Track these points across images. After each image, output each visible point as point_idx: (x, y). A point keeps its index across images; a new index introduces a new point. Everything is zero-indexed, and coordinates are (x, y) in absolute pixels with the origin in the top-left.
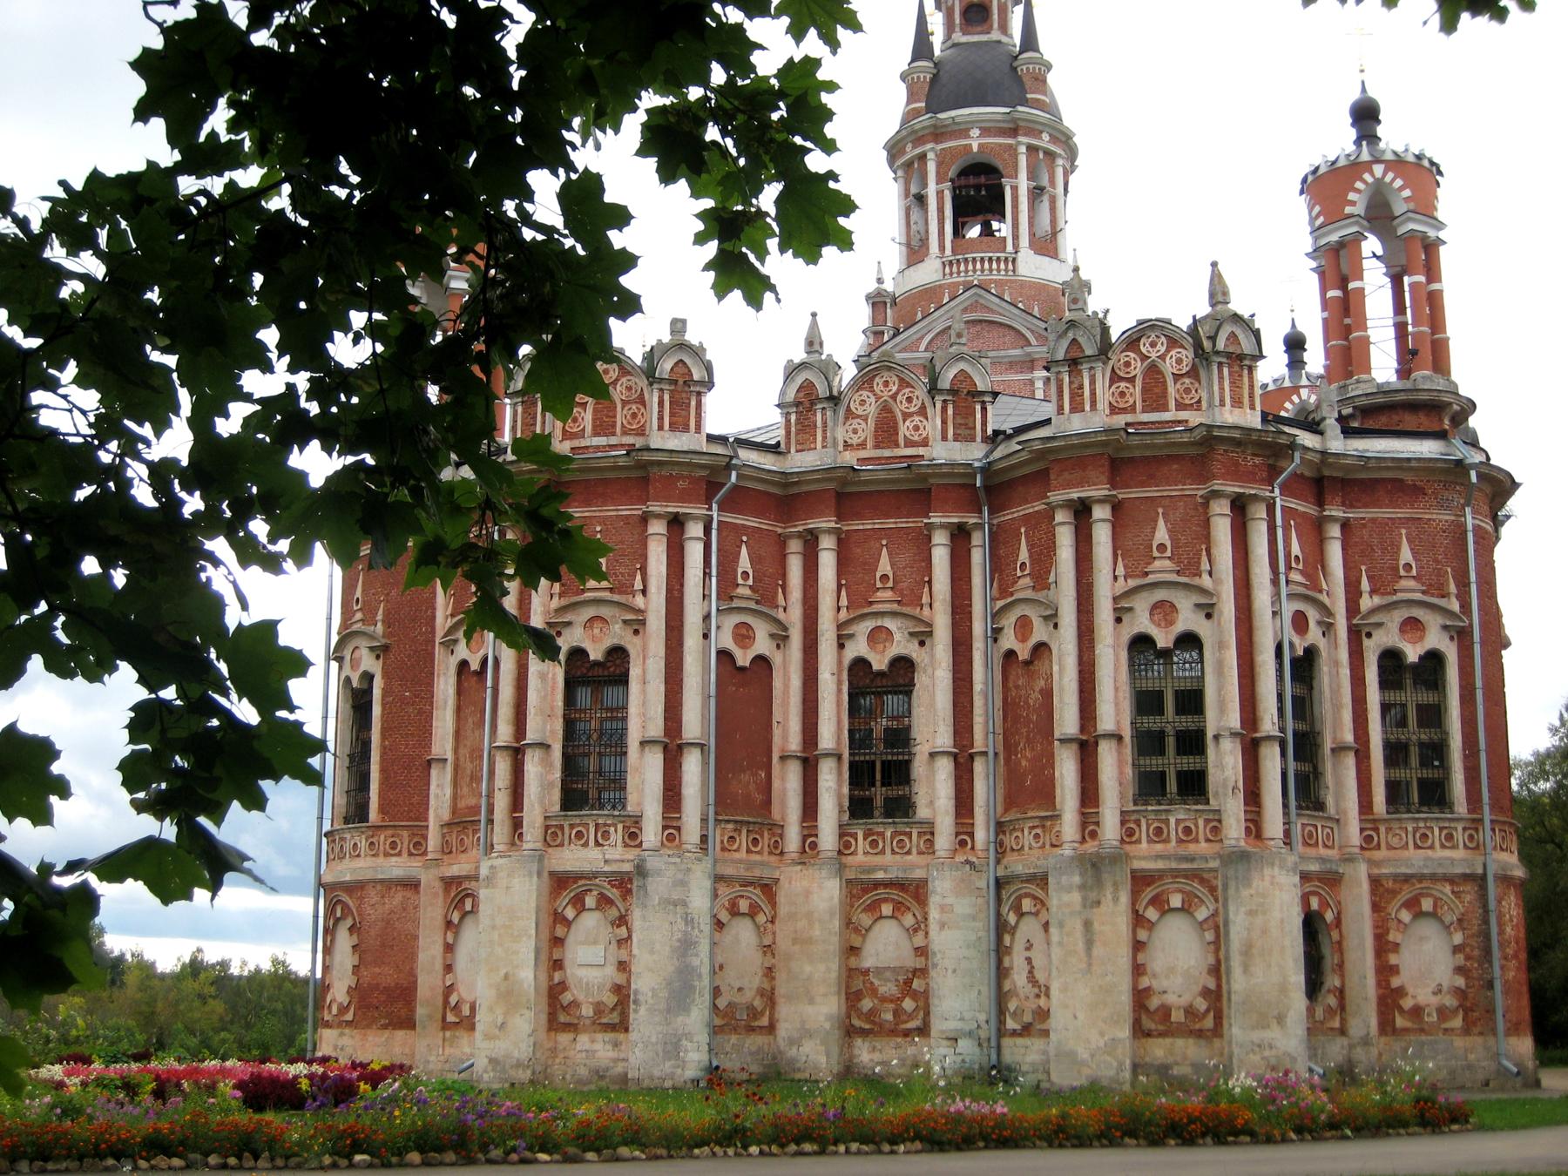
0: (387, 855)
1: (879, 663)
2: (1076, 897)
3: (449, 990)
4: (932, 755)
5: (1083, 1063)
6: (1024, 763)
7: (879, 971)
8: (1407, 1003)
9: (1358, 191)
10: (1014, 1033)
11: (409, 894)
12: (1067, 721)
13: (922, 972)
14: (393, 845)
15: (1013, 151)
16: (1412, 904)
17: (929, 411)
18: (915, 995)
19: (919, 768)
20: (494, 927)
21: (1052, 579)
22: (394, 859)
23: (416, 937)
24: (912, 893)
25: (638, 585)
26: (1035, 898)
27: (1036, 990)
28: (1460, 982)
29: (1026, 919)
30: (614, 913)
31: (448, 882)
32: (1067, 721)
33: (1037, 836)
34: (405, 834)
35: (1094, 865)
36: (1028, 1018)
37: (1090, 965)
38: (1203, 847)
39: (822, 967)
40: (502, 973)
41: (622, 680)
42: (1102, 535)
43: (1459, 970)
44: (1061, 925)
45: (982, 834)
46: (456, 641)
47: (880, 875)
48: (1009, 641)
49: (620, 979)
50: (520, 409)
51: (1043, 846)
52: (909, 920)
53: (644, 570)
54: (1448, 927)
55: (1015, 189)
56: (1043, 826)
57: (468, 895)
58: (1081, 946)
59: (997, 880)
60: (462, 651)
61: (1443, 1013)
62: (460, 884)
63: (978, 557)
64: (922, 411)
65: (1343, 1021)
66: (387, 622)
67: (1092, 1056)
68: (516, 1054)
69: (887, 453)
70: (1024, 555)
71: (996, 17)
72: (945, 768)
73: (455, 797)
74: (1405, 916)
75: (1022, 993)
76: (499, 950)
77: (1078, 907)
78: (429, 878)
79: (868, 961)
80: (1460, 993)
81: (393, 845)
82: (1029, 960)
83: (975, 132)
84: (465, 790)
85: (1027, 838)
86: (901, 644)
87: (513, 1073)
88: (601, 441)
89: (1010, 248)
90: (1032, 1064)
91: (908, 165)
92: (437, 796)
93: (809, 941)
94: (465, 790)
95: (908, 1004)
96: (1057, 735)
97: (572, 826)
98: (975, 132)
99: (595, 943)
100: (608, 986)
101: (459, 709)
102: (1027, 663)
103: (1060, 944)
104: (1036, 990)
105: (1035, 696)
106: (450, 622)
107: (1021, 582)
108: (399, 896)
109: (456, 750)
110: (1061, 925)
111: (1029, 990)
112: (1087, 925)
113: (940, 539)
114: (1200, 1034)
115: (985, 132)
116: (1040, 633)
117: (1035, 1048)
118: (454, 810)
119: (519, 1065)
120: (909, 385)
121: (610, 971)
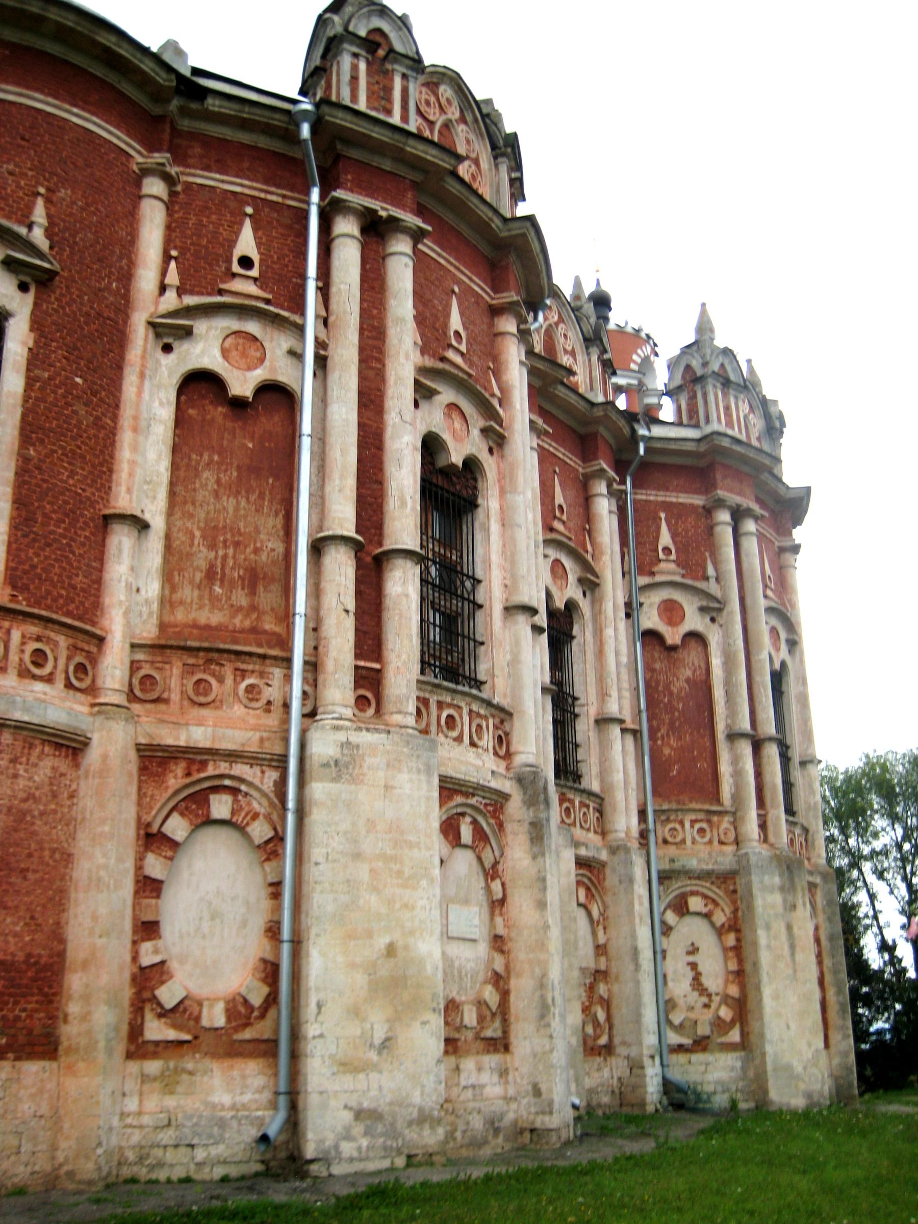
0: (24, 673)
3: (146, 979)
5: (798, 1078)
6: (667, 751)
9: (638, 355)
10: (680, 1048)
11: (63, 765)
14: (39, 658)
20: (357, 856)
21: (711, 571)
22: (39, 686)
23: (68, 858)
26: (705, 897)
27: (705, 999)
29: (688, 919)
30: (488, 857)
31: (153, 760)
33: (701, 831)
34: (63, 641)
35: (788, 867)
36: (703, 1030)
37: (795, 971)
40: (382, 941)
41: (471, 505)
44: (768, 927)
46: (188, 333)
48: (651, 619)
49: (499, 964)
50: (363, 66)
51: (710, 842)
53: (497, 374)
56: (709, 821)
57: (216, 789)
58: (786, 951)
59: (659, 872)
62: (203, 765)
65: (744, 1034)
67: (805, 1068)
68: (416, 1098)
70: (665, 539)
73: (162, 601)
75: (681, 1002)
76: (374, 900)
77: (780, 910)
78: (113, 743)
81: (39, 658)
82: (693, 966)
84: (187, 593)
85: (689, 832)
87: (412, 1135)
90: (717, 1082)
92: (129, 586)
94: (187, 593)
97: (440, 705)
99: (466, 902)
100: (481, 977)
101: (176, 449)
102: (674, 648)
103: (769, 947)
104: (705, 999)
105: (679, 685)
106: (170, 301)
107: (663, 565)
108: (46, 765)
109: (170, 513)
110: (768, 927)
111: (694, 998)
112: (789, 928)
116: (693, 621)
117: (721, 1063)
118: (163, 626)
119: (423, 1119)
120: (563, 321)
121: (483, 949)
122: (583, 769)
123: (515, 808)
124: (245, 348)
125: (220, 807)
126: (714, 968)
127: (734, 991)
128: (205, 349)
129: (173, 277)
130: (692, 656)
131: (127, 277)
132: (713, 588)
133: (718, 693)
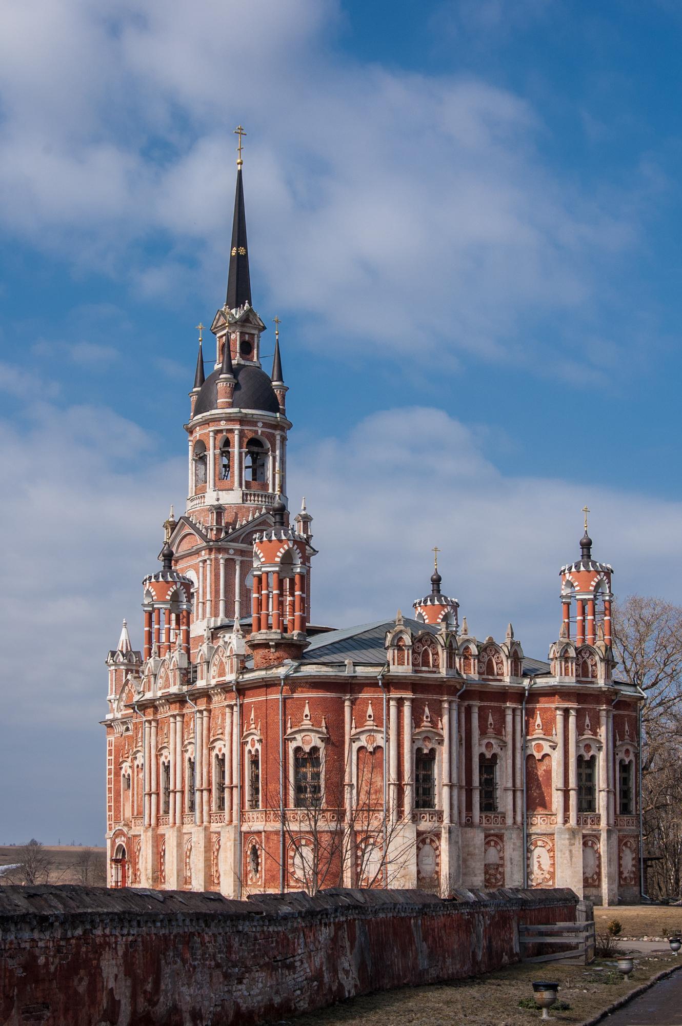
1: (488, 756)
2: (567, 842)
4: (506, 789)
7: (489, 865)
8: (624, 876)
12: (557, 781)
13: (502, 865)
15: (274, 436)
16: (625, 844)
17: (505, 663)
18: (500, 873)
19: (499, 793)
21: (554, 732)
24: (500, 837)
25: (440, 726)
28: (634, 869)
32: (557, 781)
38: (594, 827)
39: (479, 864)
42: (572, 720)
43: (633, 866)
45: (519, 819)
47: (492, 832)
52: (499, 848)
54: (632, 852)
55: (274, 458)
58: (569, 858)
60: (363, 741)
61: (631, 879)
63: (518, 719)
64: (502, 662)
66: (326, 728)
69: (491, 677)
70: (539, 721)
71: (255, 352)
72: (510, 793)
74: (624, 848)
79: (487, 862)
80: (634, 872)
83: (260, 424)
86: (496, 749)
88: (424, 669)
89: (270, 491)
91: (217, 432)
93: (474, 854)
95: (499, 876)
96: (554, 786)
98: (260, 424)
106: (354, 731)
112: (571, 851)
113: (509, 713)
114: (594, 886)
115: (265, 425)
116: (547, 749)
122: (499, 805)
123: (444, 835)
124: (372, 739)
125: (371, 841)
126: (546, 863)
127: (552, 870)
128: (363, 741)
129: (353, 725)
130: (546, 761)
131: (343, 728)
132: (554, 738)
133: (554, 774)
